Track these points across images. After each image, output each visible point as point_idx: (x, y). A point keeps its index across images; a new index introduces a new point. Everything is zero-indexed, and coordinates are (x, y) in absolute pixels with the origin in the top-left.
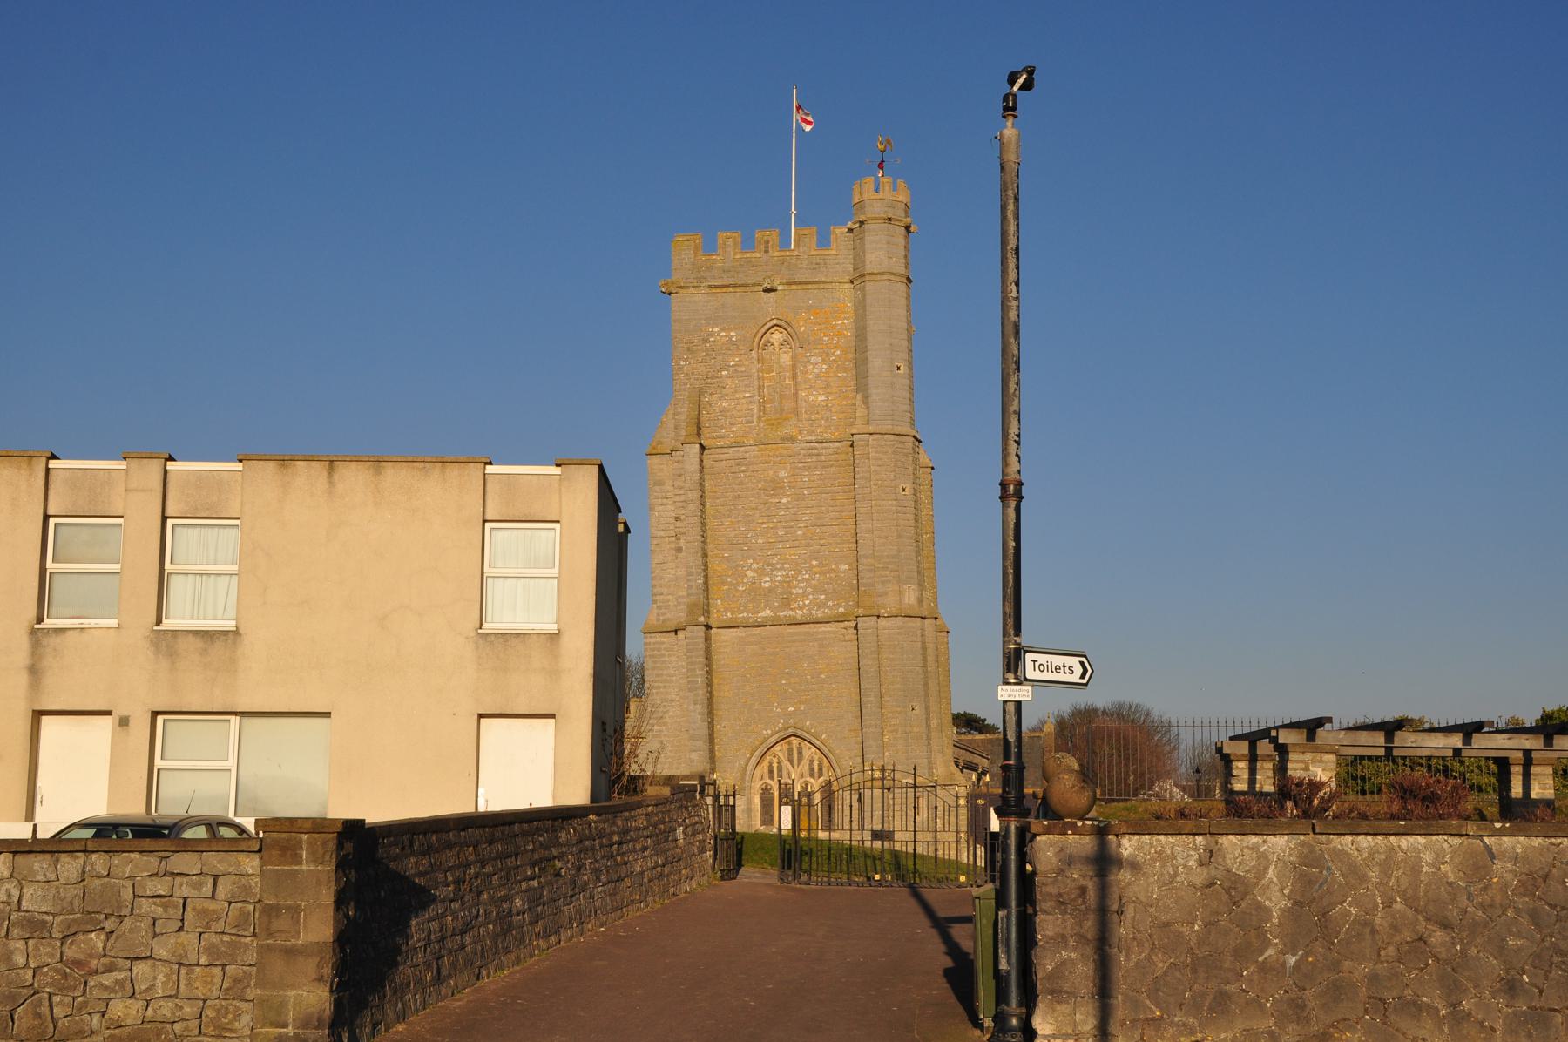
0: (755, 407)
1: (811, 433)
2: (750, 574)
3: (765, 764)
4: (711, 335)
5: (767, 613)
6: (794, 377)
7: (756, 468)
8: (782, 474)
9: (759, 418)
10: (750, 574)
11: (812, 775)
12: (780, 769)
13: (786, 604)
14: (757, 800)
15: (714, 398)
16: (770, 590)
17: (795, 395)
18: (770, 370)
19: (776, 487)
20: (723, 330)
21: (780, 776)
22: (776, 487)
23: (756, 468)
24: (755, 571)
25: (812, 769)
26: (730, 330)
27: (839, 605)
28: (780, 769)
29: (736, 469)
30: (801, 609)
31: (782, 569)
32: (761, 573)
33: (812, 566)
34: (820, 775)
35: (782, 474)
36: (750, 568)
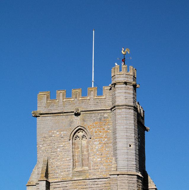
0: (71, 164)
4: (53, 133)
6: (88, 151)
9: (73, 169)
15: (54, 160)
17: (88, 158)
18: (78, 148)
20: (57, 131)
26: (61, 131)
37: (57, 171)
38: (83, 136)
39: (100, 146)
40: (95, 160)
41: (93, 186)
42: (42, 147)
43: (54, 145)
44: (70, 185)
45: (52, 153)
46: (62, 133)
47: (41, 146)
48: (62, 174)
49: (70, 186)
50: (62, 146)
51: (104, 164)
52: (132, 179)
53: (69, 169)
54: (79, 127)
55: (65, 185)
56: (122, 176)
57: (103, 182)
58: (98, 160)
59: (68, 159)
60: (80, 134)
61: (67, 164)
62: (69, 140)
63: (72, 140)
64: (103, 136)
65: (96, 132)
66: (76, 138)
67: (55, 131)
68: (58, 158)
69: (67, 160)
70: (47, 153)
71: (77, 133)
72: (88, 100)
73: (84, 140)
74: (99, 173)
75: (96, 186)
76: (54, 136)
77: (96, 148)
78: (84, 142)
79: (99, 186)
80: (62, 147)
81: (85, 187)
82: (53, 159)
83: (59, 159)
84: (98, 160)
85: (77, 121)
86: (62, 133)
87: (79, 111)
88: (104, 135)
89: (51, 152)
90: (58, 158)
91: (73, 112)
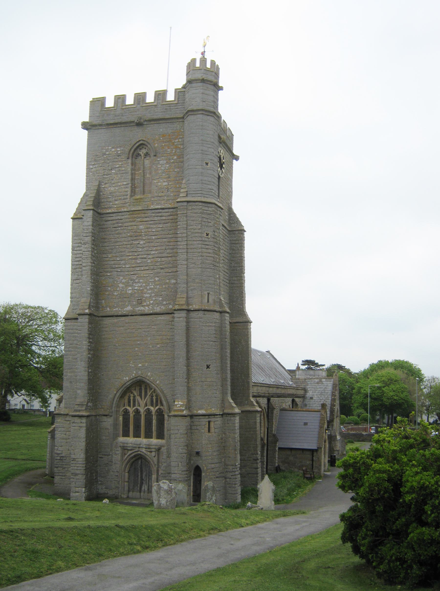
0: (129, 190)
1: (158, 204)
2: (121, 285)
3: (126, 398)
5: (129, 308)
7: (125, 225)
8: (141, 227)
9: (131, 196)
10: (121, 285)
11: (152, 405)
12: (134, 401)
13: (140, 302)
14: (121, 418)
15: (107, 185)
16: (131, 294)
18: (139, 170)
19: (137, 235)
20: (113, 148)
21: (134, 405)
22: (137, 235)
24: (123, 283)
25: (152, 401)
26: (117, 147)
27: (170, 304)
28: (134, 401)
29: (115, 226)
30: (148, 306)
31: (139, 282)
32: (127, 285)
33: (155, 281)
34: (157, 405)
35: (141, 227)
36: (121, 282)
37: (110, 200)
38: (147, 155)
39: (167, 166)
40: (159, 184)
41: (156, 219)
42: (92, 168)
43: (107, 165)
44: (126, 216)
45: (105, 176)
46: (119, 149)
48: (117, 202)
49: (126, 219)
50: (118, 166)
51: (171, 190)
52: (206, 209)
53: (125, 197)
54: (141, 142)
55: (119, 217)
56: (194, 204)
59: (125, 183)
60: (143, 152)
61: (124, 189)
62: (128, 158)
63: (130, 158)
66: (137, 156)
67: (110, 148)
68: (113, 182)
69: (123, 185)
71: (138, 150)
73: (148, 159)
74: (163, 202)
75: (159, 218)
76: (108, 154)
77: (163, 168)
78: (147, 162)
79: (164, 218)
80: (118, 167)
82: (106, 184)
83: (114, 184)
85: (137, 135)
86: (119, 149)
87: (142, 121)
88: (174, 152)
89: (104, 175)
91: (133, 122)
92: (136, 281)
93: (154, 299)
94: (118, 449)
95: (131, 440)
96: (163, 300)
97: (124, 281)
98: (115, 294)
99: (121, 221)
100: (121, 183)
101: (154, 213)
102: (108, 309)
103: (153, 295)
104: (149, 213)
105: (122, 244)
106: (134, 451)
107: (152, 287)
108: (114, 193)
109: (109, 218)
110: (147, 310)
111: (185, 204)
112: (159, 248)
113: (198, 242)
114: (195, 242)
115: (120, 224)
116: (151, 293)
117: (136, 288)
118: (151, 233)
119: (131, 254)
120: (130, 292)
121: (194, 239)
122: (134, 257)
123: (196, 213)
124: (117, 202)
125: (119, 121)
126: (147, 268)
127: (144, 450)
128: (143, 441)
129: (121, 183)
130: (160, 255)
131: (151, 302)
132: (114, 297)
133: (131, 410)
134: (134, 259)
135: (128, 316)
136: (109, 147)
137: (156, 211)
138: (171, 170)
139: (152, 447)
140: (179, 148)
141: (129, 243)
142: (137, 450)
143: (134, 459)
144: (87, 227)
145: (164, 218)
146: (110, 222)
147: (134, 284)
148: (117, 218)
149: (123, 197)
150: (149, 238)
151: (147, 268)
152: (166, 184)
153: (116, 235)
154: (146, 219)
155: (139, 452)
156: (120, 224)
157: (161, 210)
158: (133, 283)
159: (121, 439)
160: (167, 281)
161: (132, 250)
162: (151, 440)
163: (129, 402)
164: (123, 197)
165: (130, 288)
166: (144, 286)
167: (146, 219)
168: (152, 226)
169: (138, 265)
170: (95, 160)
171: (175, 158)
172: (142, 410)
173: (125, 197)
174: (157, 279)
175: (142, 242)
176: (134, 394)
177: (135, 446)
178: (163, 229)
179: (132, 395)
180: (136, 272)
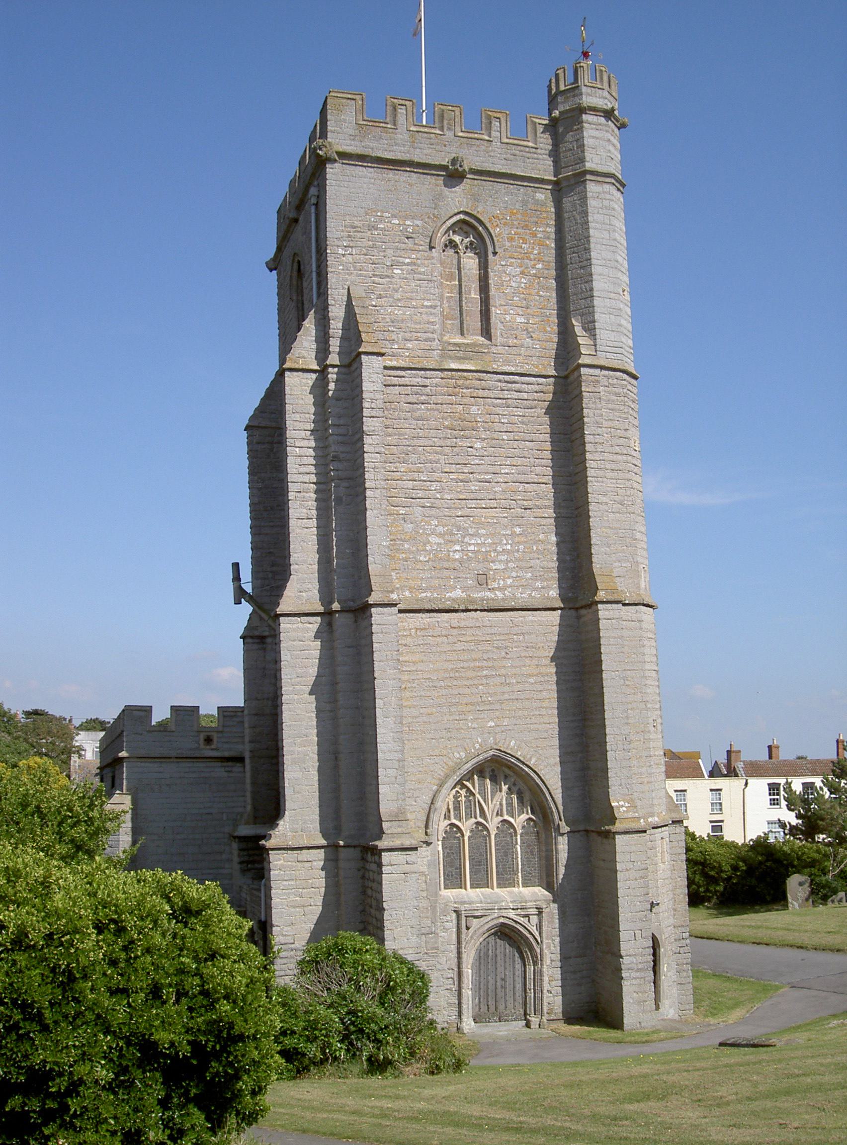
1: (507, 362)
2: (434, 539)
5: (458, 593)
20: (394, 216)
23: (440, 399)
24: (440, 535)
29: (411, 399)
30: (500, 589)
33: (513, 534)
37: (394, 337)
40: (508, 318)
42: (344, 255)
43: (382, 254)
44: (435, 381)
45: (377, 279)
46: (408, 223)
47: (341, 251)
48: (409, 345)
50: (408, 260)
53: (430, 335)
54: (462, 216)
57: (537, 388)
58: (519, 320)
59: (426, 303)
60: (457, 239)
62: (431, 248)
64: (532, 253)
65: (511, 239)
68: (397, 296)
69: (423, 306)
70: (360, 275)
72: (485, 143)
74: (519, 359)
75: (516, 395)
77: (514, 284)
79: (525, 396)
80: (408, 264)
81: (481, 393)
83: (399, 300)
84: (519, 320)
85: (457, 199)
86: (408, 223)
89: (374, 275)
90: (397, 296)
92: (471, 531)
93: (514, 574)
94: (449, 918)
95: (472, 896)
96: (535, 578)
97: (440, 529)
98: (421, 559)
99: (428, 390)
100: (420, 303)
101: (500, 381)
102: (407, 593)
103: (511, 565)
104: (492, 380)
105: (431, 443)
106: (490, 918)
107: (509, 547)
108: (403, 321)
109: (395, 380)
110: (498, 596)
111: (597, 372)
112: (519, 461)
113: (624, 457)
114: (620, 457)
115: (423, 398)
116: (507, 562)
117: (472, 548)
118: (497, 426)
119: (453, 468)
120: (457, 556)
121: (617, 449)
122: (461, 477)
123: (617, 395)
124: (409, 345)
125: (406, 157)
126: (493, 503)
127: (512, 914)
128: (503, 893)
129: (420, 303)
130: (522, 478)
131: (509, 581)
132: (419, 566)
133: (467, 826)
134: (462, 481)
135: (456, 611)
136: (383, 212)
137: (507, 378)
138: (534, 292)
139: (529, 904)
140: (547, 245)
141: (448, 442)
142: (496, 915)
143: (486, 935)
144: (372, 395)
145: (525, 396)
146: (397, 388)
147: (467, 539)
148: (415, 381)
149: (425, 336)
150: (495, 436)
151: (493, 503)
152: (523, 320)
153: (414, 422)
154: (486, 393)
155: (502, 920)
156: (423, 398)
157: (517, 378)
158: (463, 537)
159: (450, 894)
160: (541, 536)
161: (458, 459)
162: (515, 890)
163: (457, 808)
164: (425, 336)
165: (458, 548)
166: (490, 545)
167: (486, 393)
168: (499, 410)
169: (472, 496)
170: (349, 236)
171: (540, 266)
172: (493, 824)
173: (430, 335)
174: (518, 530)
175: (478, 445)
176: (468, 790)
177: (490, 906)
178: (525, 419)
179: (463, 792)
180: (467, 512)
